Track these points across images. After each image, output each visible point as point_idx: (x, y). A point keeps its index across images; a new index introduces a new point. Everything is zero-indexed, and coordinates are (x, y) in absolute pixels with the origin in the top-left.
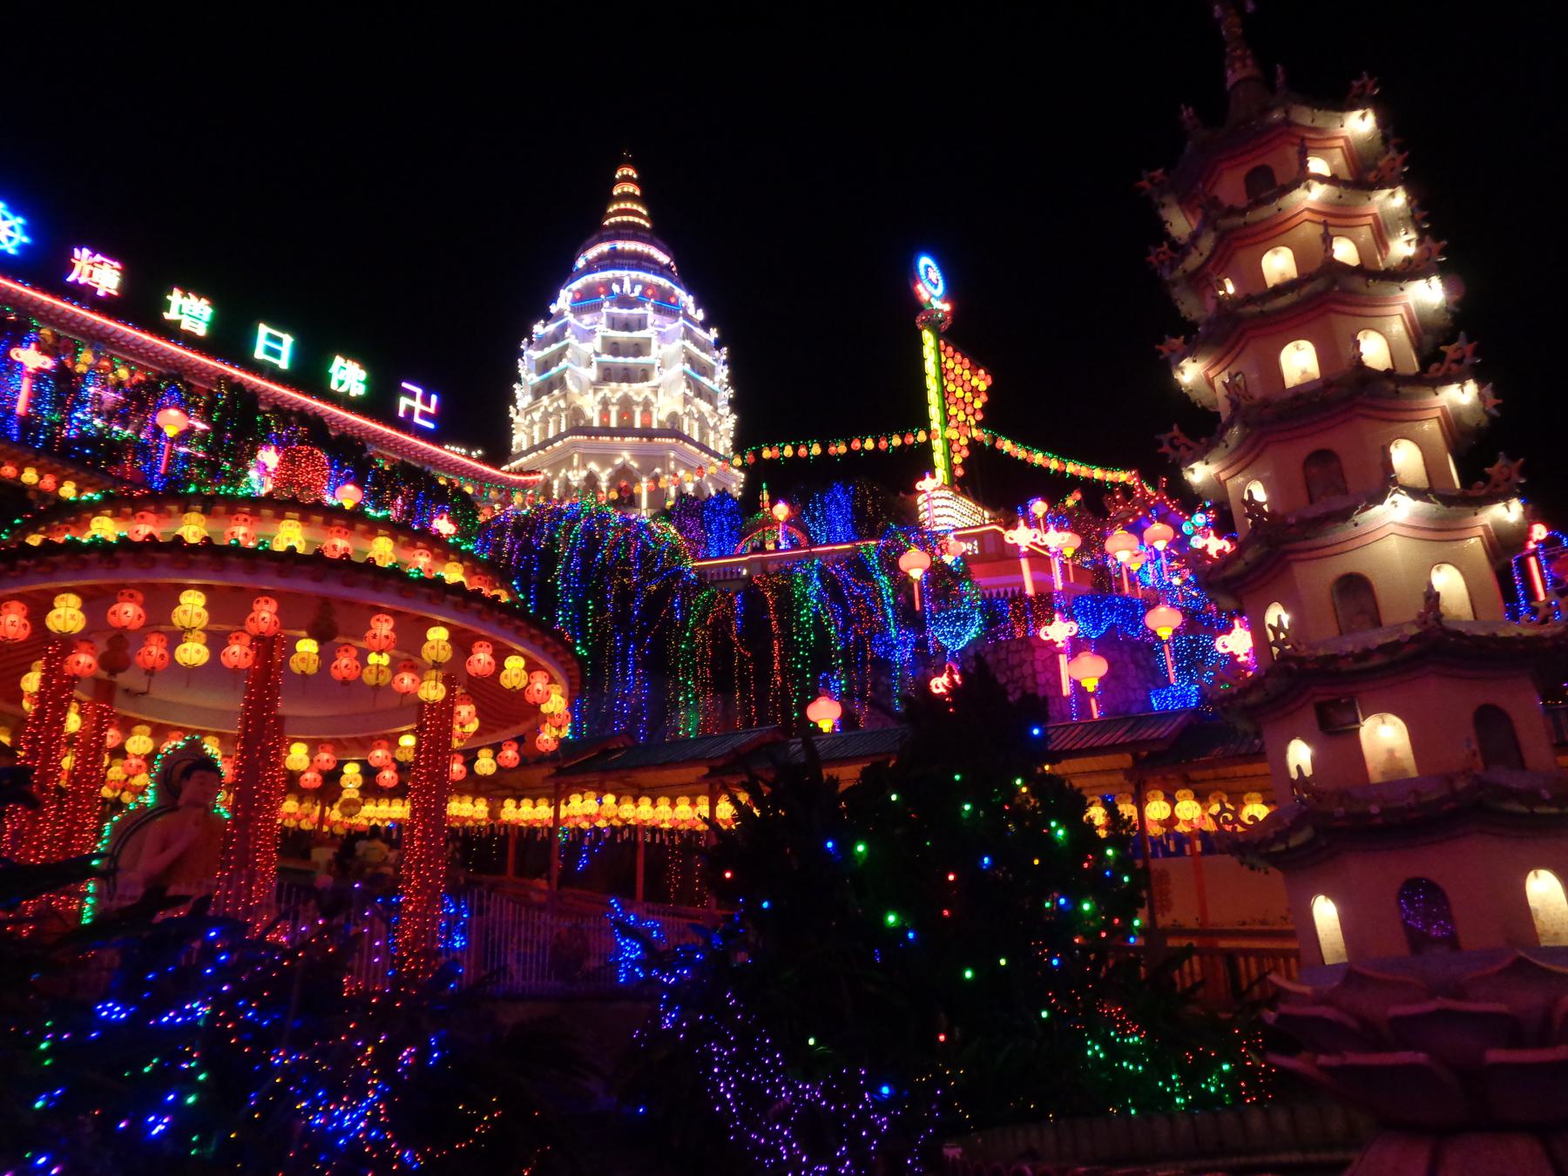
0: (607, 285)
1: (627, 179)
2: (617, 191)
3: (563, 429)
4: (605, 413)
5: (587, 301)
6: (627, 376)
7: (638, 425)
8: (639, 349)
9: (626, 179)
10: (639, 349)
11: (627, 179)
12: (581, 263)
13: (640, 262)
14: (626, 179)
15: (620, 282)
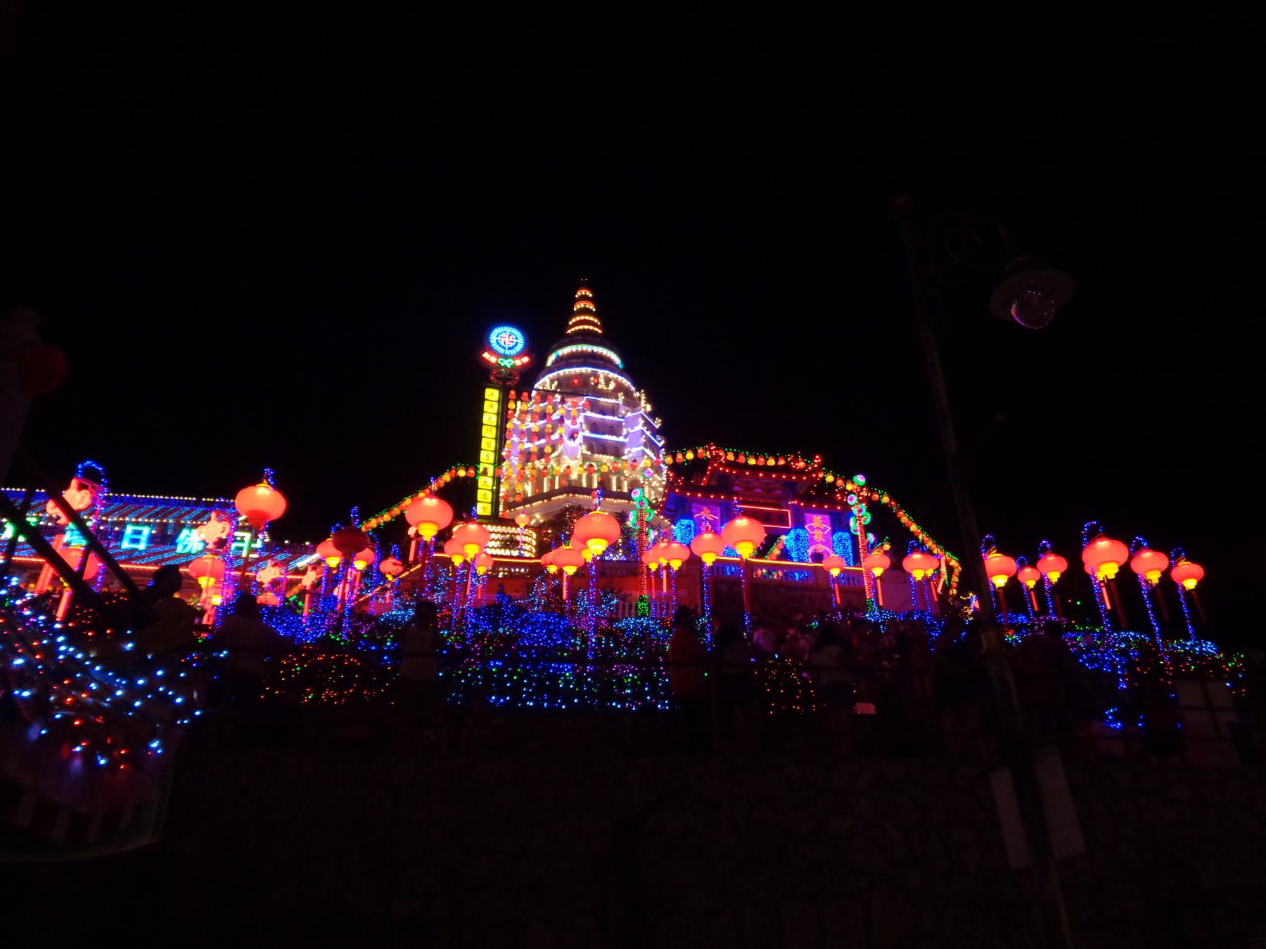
0: (584, 379)
1: (584, 298)
2: (579, 305)
3: (557, 487)
4: (590, 479)
5: (570, 389)
6: (604, 448)
7: (614, 489)
8: (614, 429)
9: (584, 300)
10: (614, 429)
11: (584, 298)
12: (551, 360)
13: (606, 363)
14: (584, 300)
15: (596, 376)
